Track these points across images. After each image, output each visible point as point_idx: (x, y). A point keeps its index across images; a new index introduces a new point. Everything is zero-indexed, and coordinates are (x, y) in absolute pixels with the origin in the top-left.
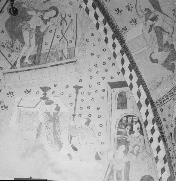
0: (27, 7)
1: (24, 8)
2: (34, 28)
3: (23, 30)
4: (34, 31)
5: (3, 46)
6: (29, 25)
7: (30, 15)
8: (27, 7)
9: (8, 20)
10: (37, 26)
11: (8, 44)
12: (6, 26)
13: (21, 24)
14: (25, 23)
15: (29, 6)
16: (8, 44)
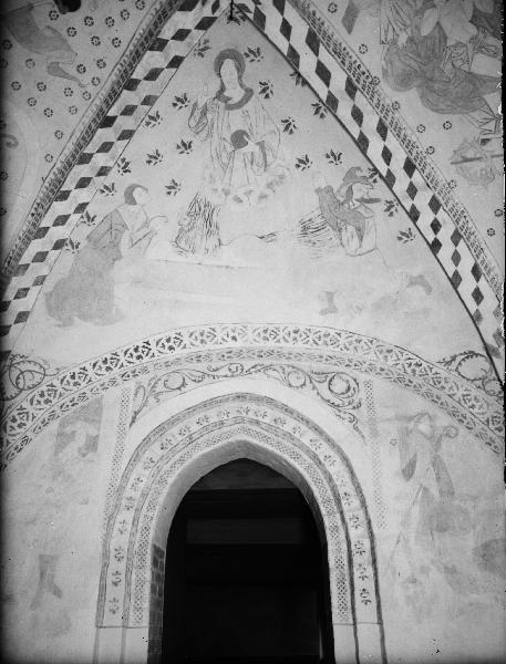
0: (409, 30)
1: (411, 40)
2: (473, 30)
3: (465, 67)
4: (481, 35)
5: (484, 141)
6: (459, 44)
7: (432, 31)
8: (409, 30)
9: (422, 96)
10: (471, 21)
11: (486, 127)
12: (437, 111)
13: (449, 66)
14: (449, 52)
15: (408, 22)
16: (486, 127)
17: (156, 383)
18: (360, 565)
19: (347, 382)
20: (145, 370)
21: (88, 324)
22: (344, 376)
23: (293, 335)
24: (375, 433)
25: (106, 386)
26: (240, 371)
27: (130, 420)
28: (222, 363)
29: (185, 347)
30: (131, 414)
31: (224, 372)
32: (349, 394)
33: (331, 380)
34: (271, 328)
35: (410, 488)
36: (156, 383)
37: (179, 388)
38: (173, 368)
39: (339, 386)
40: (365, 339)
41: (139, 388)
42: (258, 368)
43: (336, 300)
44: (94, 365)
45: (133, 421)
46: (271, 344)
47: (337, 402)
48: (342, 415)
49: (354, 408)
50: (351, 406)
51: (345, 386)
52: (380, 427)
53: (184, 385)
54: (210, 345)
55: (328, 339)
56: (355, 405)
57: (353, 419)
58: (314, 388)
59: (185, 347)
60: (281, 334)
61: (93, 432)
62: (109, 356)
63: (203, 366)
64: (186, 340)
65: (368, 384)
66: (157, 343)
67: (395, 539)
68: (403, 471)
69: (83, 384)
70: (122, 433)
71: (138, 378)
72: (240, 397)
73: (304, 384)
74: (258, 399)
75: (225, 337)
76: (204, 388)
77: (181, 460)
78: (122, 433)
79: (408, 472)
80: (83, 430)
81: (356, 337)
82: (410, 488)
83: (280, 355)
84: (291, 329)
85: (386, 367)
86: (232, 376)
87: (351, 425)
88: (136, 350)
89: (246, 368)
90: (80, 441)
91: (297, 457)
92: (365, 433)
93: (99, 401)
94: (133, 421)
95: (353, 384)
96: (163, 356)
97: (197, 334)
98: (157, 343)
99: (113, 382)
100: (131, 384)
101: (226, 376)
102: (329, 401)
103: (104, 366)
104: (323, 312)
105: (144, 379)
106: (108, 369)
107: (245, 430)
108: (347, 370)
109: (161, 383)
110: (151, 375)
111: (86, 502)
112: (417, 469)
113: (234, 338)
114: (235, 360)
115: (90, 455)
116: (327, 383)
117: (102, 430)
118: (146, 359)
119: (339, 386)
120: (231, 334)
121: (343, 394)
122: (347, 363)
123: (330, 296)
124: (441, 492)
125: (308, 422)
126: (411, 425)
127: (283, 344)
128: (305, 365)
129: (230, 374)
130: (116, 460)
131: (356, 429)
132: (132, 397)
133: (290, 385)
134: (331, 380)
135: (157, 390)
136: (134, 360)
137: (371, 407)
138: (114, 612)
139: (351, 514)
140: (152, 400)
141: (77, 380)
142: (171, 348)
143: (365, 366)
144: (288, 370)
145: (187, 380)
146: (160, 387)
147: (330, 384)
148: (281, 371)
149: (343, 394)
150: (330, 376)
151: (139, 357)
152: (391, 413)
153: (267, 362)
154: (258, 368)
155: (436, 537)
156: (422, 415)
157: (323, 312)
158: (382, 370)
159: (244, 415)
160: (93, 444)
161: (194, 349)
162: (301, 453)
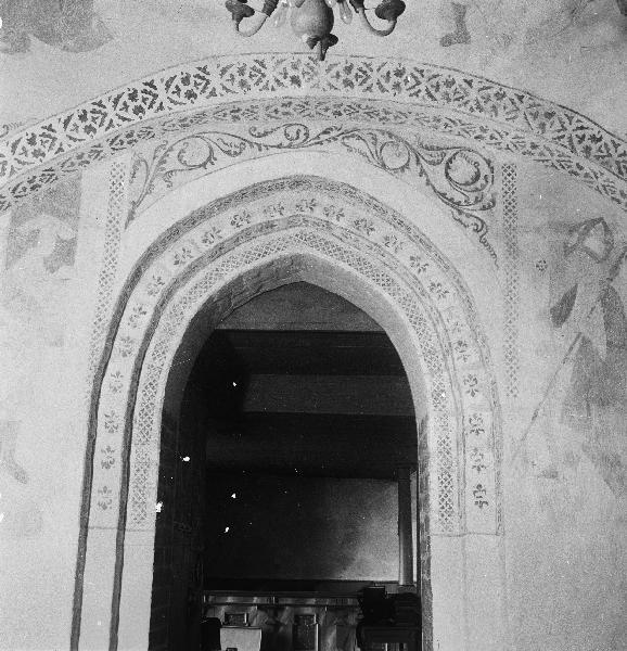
17: (166, 155)
19: (476, 164)
20: (148, 133)
21: (54, 51)
22: (470, 154)
23: (394, 79)
24: (513, 249)
25: (86, 158)
26: (302, 137)
27: (125, 218)
28: (272, 124)
29: (213, 93)
30: (126, 208)
31: (278, 137)
32: (478, 185)
33: (450, 161)
34: (358, 63)
35: (563, 338)
36: (166, 155)
37: (204, 165)
38: (196, 129)
39: (462, 171)
40: (510, 94)
41: (138, 162)
42: (333, 134)
43: (469, 18)
44: (66, 123)
45: (131, 217)
46: (357, 93)
47: (458, 197)
48: (463, 218)
49: (484, 208)
50: (479, 205)
51: (472, 170)
52: (524, 240)
53: (211, 159)
54: (255, 92)
55: (450, 91)
56: (486, 201)
57: (481, 228)
58: (422, 173)
59: (213, 93)
60: (375, 76)
61: (67, 235)
62: (89, 108)
63: (241, 128)
64: (216, 81)
65: (509, 170)
66: (168, 86)
69: (50, 155)
70: (113, 234)
71: (136, 147)
72: (297, 183)
73: (407, 166)
74: (331, 187)
75: (280, 78)
76: (247, 165)
77: (207, 281)
78: (113, 234)
79: (560, 314)
80: (49, 229)
81: (496, 89)
82: (563, 338)
83: (371, 113)
84: (392, 67)
85: (541, 143)
86: (289, 146)
88: (133, 97)
89: (313, 134)
90: (46, 247)
91: (388, 283)
93: (75, 185)
94: (131, 217)
95: (485, 170)
96: (176, 108)
97: (234, 71)
98: (168, 86)
99: (96, 152)
100: (125, 158)
101: (279, 146)
102: (444, 195)
103: (82, 125)
104: (446, 41)
105: (146, 148)
106: (89, 129)
107: (302, 237)
108: (478, 145)
109: (174, 155)
110: (156, 142)
111: (59, 342)
112: (577, 306)
113: (295, 80)
114: (296, 117)
115: (63, 271)
116: (443, 166)
117: (80, 232)
118: (150, 113)
119: (462, 171)
120: (292, 73)
121: (467, 184)
122: (478, 133)
123: (460, 13)
124: (609, 344)
125: (408, 229)
126: (573, 240)
127: (376, 93)
128: (408, 132)
129: (286, 143)
130: (105, 277)
131: (485, 243)
132: (127, 177)
133: (384, 166)
134: (450, 161)
135: (168, 167)
136: (130, 114)
137: (510, 208)
138: (105, 508)
139: (465, 373)
140: (160, 184)
141: (38, 146)
142: (190, 95)
143: (508, 139)
144: (382, 139)
145: (218, 154)
146: (172, 163)
147: (448, 167)
148: (368, 138)
149: (467, 184)
150: (450, 153)
151: (139, 110)
152: (541, 220)
153: (349, 124)
154: (333, 134)
155: (593, 413)
156: (594, 222)
157: (446, 41)
158: (534, 146)
159: (307, 212)
160: (66, 251)
161: (230, 98)
162: (393, 275)
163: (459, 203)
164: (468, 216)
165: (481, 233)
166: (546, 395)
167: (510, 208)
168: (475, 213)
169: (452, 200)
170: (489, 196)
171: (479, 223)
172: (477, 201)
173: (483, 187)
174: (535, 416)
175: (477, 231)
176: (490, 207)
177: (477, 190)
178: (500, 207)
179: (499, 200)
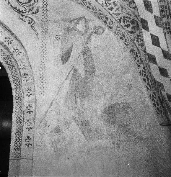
18: (28, 120)
24: (45, 31)
32: (31, 3)
35: (66, 69)
47: (22, 9)
48: (24, 18)
49: (33, 13)
52: (50, 26)
56: (34, 11)
67: (50, 102)
68: (62, 57)
79: (65, 58)
82: (66, 69)
87: (30, 25)
92: (38, 31)
102: (16, 8)
112: (72, 56)
124: (86, 71)
126: (71, 26)
131: (32, 28)
137: (45, 14)
149: (26, 3)
152: (59, 17)
155: (78, 101)
156: (81, 18)
163: (22, 11)
164: (26, 17)
165: (31, 24)
166: (57, 94)
167: (45, 14)
168: (29, 16)
169: (19, 10)
170: (35, 8)
171: (31, 20)
172: (30, 10)
173: (33, 4)
174: (51, 104)
175: (29, 23)
176: (36, 13)
177: (30, 5)
178: (40, 14)
179: (40, 9)
